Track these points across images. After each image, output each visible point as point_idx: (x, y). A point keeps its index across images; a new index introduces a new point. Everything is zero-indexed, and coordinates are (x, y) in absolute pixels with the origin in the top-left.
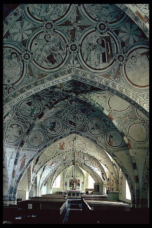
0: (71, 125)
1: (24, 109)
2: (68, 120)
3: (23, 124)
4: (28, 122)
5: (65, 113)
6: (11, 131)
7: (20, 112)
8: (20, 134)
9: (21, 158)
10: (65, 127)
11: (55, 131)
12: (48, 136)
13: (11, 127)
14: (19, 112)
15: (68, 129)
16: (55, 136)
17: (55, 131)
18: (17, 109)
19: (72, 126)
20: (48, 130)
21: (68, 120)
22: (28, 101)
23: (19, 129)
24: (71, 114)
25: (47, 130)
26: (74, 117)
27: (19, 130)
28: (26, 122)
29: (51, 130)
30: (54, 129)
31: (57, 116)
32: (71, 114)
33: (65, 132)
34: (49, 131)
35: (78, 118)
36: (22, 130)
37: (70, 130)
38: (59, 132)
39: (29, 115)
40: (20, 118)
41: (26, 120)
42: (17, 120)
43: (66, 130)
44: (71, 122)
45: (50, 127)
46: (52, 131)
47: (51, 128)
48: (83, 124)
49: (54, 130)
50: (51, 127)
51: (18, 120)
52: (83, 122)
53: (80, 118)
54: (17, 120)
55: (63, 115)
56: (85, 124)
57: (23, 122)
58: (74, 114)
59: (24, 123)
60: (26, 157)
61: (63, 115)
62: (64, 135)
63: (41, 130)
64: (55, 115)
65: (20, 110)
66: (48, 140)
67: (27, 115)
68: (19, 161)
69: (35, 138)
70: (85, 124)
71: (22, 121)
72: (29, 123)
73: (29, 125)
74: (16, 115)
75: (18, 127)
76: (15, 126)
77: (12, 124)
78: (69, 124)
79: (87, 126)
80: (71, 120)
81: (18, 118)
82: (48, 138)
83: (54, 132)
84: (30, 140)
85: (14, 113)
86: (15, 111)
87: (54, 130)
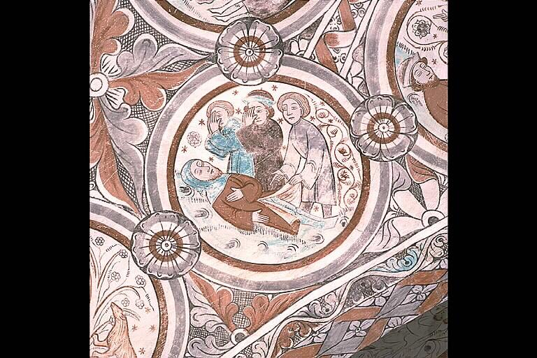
10: (395, 170)
12: (206, 290)
16: (293, 284)
20: (203, 214)
21: (415, 86)
25: (181, 218)
29: (235, 213)
30: (263, 209)
31: (281, 46)
33: (404, 226)
34: (219, 232)
38: (329, 236)
43: (404, 200)
45: (217, 189)
47: (238, 194)
49: (275, 221)
50: (236, 180)
55: (350, 27)
61: (350, 27)
62: (399, 256)
63: (118, 218)
64: (249, 22)
66: (199, 333)
82: (206, 317)
83: (270, 235)
87: (275, 221)
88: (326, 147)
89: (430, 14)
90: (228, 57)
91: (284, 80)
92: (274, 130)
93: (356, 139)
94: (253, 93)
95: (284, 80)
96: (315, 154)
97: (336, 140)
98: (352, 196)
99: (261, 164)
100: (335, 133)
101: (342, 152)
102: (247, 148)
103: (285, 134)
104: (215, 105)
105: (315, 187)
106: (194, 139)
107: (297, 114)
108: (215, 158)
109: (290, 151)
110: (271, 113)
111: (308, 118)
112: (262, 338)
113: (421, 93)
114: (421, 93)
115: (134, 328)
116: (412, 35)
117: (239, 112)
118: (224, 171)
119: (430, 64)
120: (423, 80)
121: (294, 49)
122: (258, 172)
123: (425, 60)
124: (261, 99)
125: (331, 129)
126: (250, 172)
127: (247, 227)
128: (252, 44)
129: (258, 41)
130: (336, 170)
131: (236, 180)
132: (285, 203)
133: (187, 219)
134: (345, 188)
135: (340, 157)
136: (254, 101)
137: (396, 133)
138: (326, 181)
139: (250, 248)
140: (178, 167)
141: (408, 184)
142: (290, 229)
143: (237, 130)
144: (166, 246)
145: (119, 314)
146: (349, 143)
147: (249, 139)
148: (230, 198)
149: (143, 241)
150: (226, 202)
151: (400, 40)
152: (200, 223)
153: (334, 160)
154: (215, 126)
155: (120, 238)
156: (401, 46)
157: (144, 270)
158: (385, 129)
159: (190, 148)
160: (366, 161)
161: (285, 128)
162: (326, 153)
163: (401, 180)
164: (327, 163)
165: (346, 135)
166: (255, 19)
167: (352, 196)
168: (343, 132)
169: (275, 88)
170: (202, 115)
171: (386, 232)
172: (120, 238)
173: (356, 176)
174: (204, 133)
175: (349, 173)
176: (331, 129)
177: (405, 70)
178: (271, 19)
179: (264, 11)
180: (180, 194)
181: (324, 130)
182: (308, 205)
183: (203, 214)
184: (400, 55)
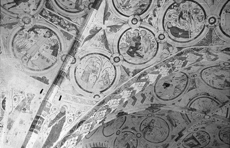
0: (177, 39)
2: (168, 28)
3: (62, 31)
4: (73, 25)
5: (158, 9)
6: (32, 41)
8: (55, 54)
9: (53, 117)
11: (141, 57)
13: (32, 29)
15: (170, 48)
17: (141, 57)
19: (181, 39)
20: (124, 54)
21: (168, 28)
23: (53, 40)
24: (170, 8)
25: (120, 54)
26: (181, 16)
27: (53, 44)
28: (68, 26)
29: (131, 54)
30: (137, 53)
31: (141, 20)
32: (170, 8)
34: (127, 57)
35: (189, 13)
36: (61, 44)
37: (176, 50)
39: (73, 6)
40: (54, 15)
41: (69, 18)
42: (48, 20)
44: (175, 31)
45: (127, 49)
46: (134, 57)
47: (132, 50)
48: (207, 26)
49: (139, 55)
51: (51, 20)
52: (205, 18)
53: (196, 13)
54: (48, 20)
56: (212, 24)
57: (62, 26)
58: (178, 5)
59: (65, 28)
60: (67, 115)
61: (155, 16)
62: (164, 62)
67: (69, 6)
68: (46, 126)
69: (94, 71)
70: (212, 24)
71: (59, 23)
72: (75, 26)
73: (75, 32)
74: (46, 6)
75: (51, 35)
76: (42, 32)
78: (173, 37)
79: (218, 27)
80: (174, 25)
81: (50, 14)
83: (138, 58)
84: (81, 75)
87: (139, 55)
88: (150, 41)
89: (171, 13)
90: (130, 22)
91: (141, 27)
92: (139, 38)
93: (156, 39)
94: (135, 30)
95: (141, 27)
96: (147, 42)
97: (152, 39)
98: (155, 50)
99: (136, 44)
100: (152, 38)
101: (153, 42)
102: (134, 41)
103: (142, 39)
104: (128, 32)
105: (147, 49)
106: (123, 38)
107: (144, 34)
108: (127, 43)
109: (142, 41)
110: (139, 34)
111: (146, 35)
112: (135, 77)
113: (169, 29)
114: (169, 29)
115: (110, 75)
116: (168, 17)
117: (132, 34)
118: (129, 45)
119: (171, 23)
120: (170, 27)
121: (144, 21)
122: (136, 46)
123: (170, 23)
124: (137, 31)
125: (151, 37)
126: (134, 46)
127: (133, 56)
128: (135, 20)
129: (136, 19)
130: (152, 45)
131: (131, 47)
132: (141, 52)
133: (121, 55)
134: (153, 49)
135: (152, 42)
136: (135, 32)
137: (164, 38)
138: (150, 48)
139: (133, 60)
140: (120, 44)
141: (166, 48)
142: (142, 57)
143: (132, 37)
144: (117, 60)
145: (107, 72)
146: (154, 40)
147: (134, 39)
148: (130, 51)
149: (112, 59)
150: (129, 51)
151: (165, 18)
152: (124, 55)
153: (151, 43)
154: (127, 37)
155: (108, 58)
156: (165, 20)
157: (112, 64)
158: (162, 37)
159: (122, 41)
160: (158, 43)
161: (142, 37)
162: (150, 42)
163: (165, 48)
164: (150, 44)
165: (154, 38)
166: (135, 15)
167: (155, 50)
168: (153, 38)
169: (140, 29)
170: (125, 34)
171: (161, 57)
172: (108, 58)
173: (156, 46)
174: (125, 38)
175: (154, 46)
176: (151, 37)
177: (166, 25)
178: (139, 15)
179: (138, 13)
180: (120, 50)
181: (149, 37)
182: (145, 52)
183: (124, 54)
184: (165, 22)
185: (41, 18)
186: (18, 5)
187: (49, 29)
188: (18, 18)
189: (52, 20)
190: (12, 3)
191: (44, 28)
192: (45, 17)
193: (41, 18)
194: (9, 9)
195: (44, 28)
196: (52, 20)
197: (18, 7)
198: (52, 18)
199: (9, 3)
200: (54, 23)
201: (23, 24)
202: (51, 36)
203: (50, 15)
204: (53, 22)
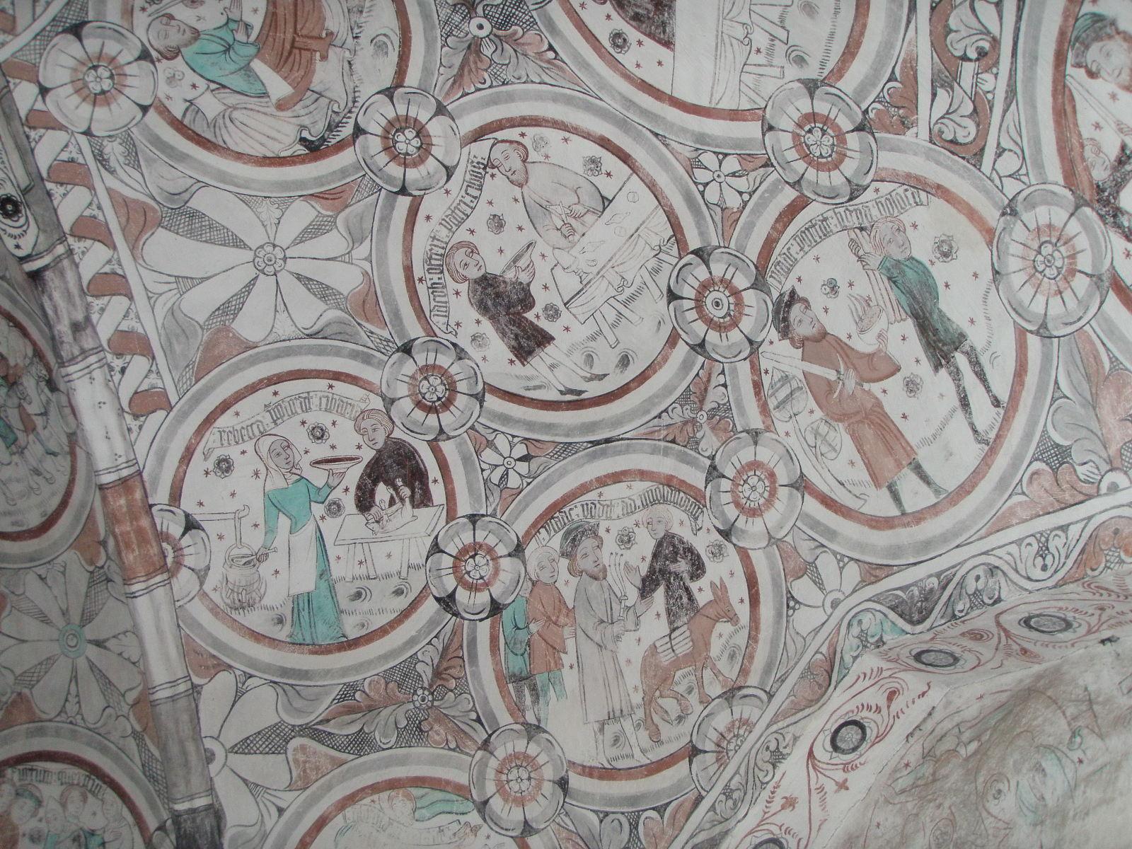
1: (760, 39)
7: (839, 72)
14: (849, 83)
18: (821, 144)
22: (619, 40)
42: (994, 84)
54: (994, 84)
65: (812, 87)
74: (905, 125)
77: (1054, 172)
81: (946, 79)
85: (887, 160)
86: (849, 167)
185: (1000, 152)
186: (962, 336)
187: (1060, 59)
188: (1043, 331)
189: (982, 54)
190: (956, 375)
191: (1064, 110)
192: (980, 113)
193: (1006, 143)
194: (996, 403)
195: (1064, 110)
196: (982, 54)
197: (976, 337)
198: (965, 58)
199: (965, 403)
200: (995, 29)
201: (1081, 284)
202: (1113, 23)
203: (956, 77)
204: (996, 42)
